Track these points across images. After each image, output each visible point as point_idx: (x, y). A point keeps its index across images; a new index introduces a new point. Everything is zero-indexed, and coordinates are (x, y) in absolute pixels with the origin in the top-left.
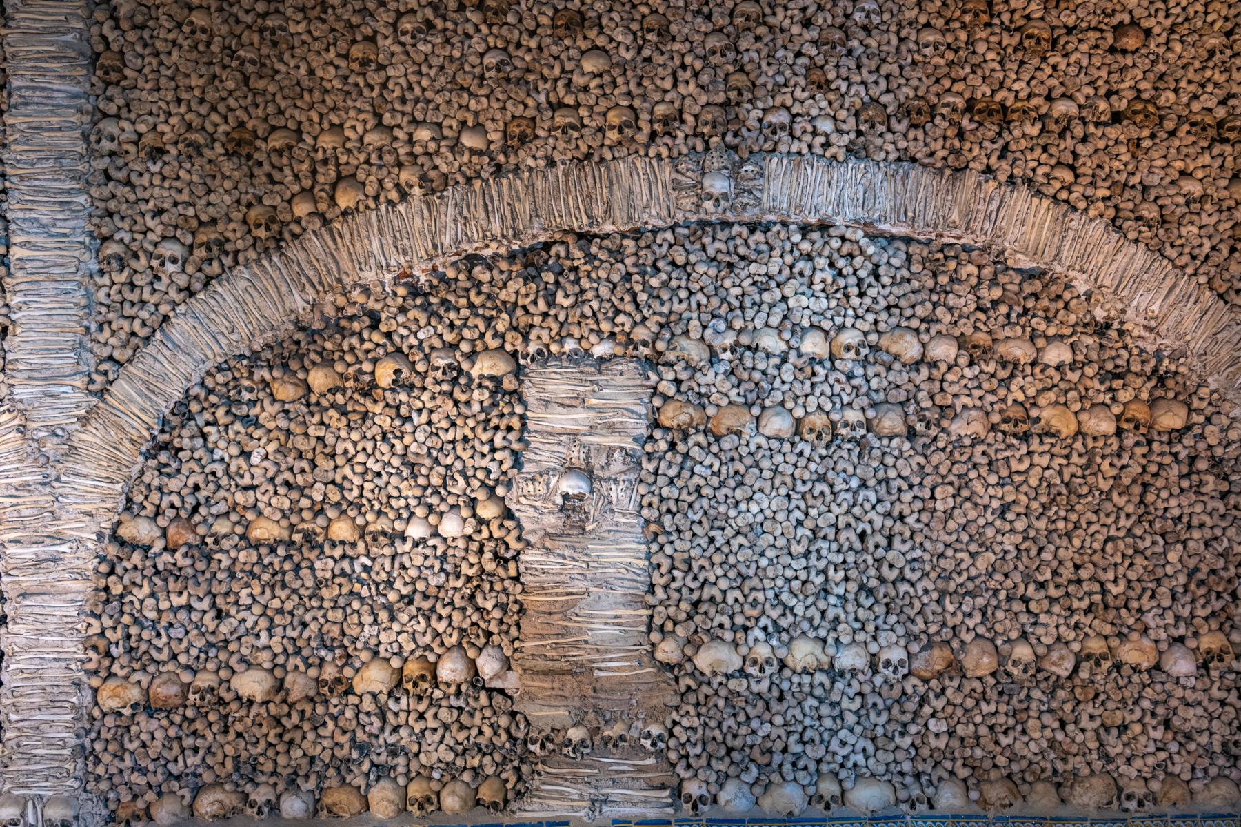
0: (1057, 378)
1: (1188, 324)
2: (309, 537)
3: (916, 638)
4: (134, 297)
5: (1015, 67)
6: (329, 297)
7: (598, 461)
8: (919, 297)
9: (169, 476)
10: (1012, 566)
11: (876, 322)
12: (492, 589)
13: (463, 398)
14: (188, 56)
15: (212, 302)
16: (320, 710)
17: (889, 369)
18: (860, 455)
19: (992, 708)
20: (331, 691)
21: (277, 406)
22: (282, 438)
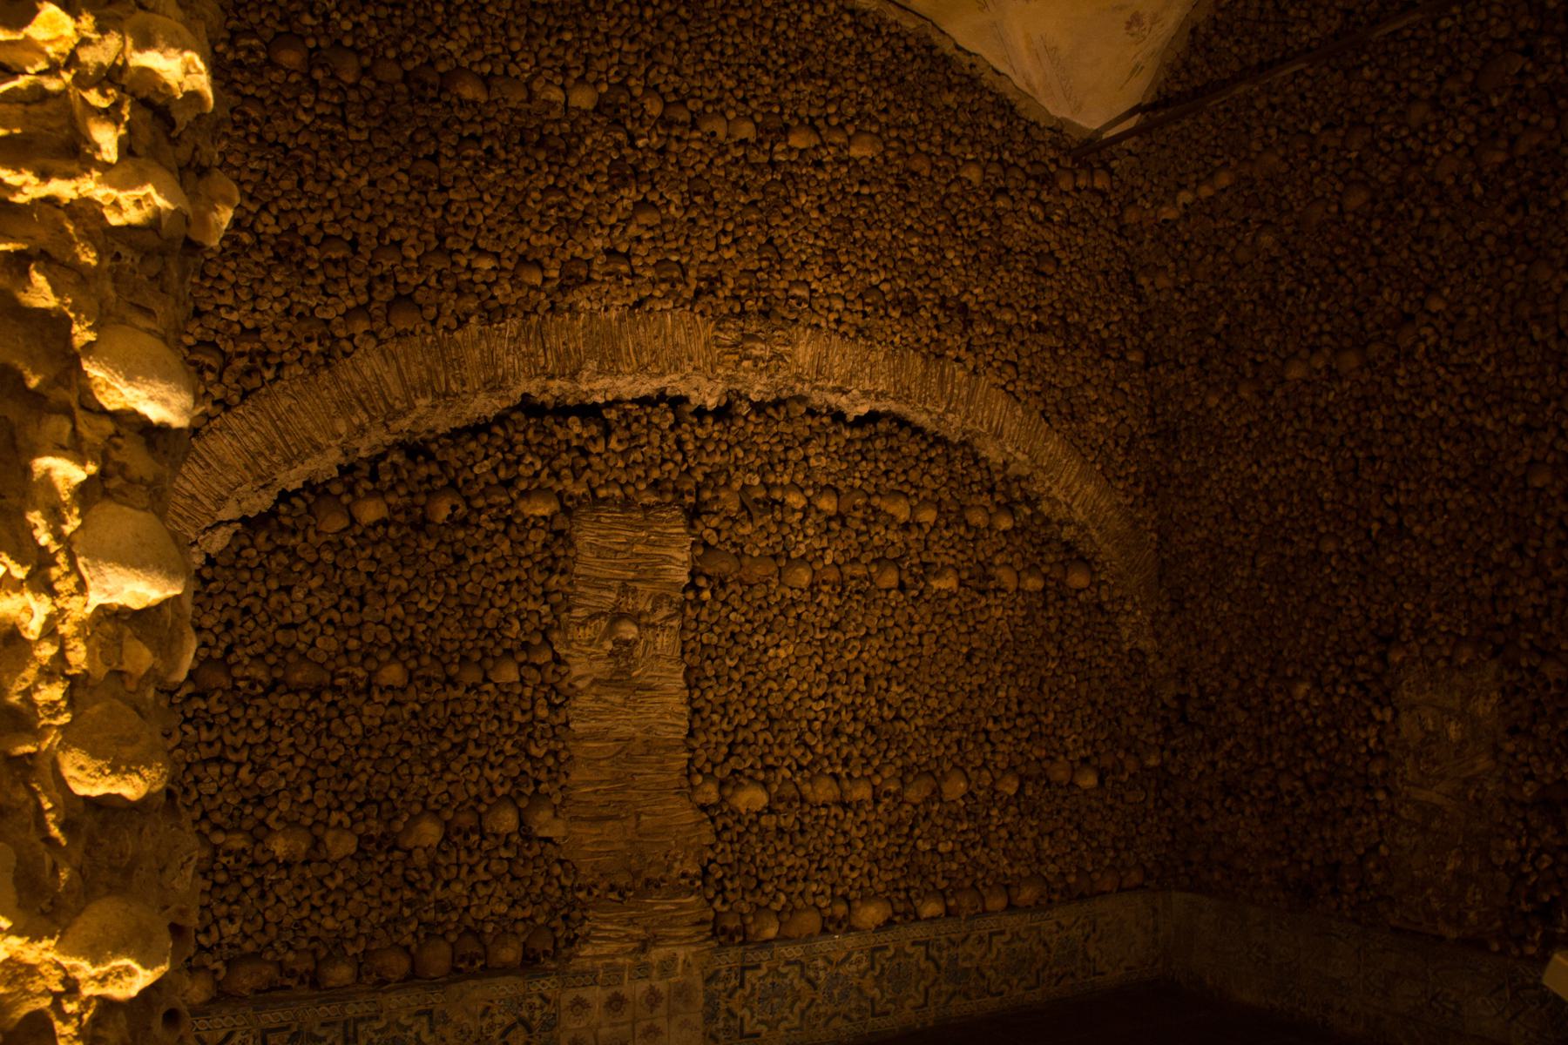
15: (253, 418)
19: (965, 827)
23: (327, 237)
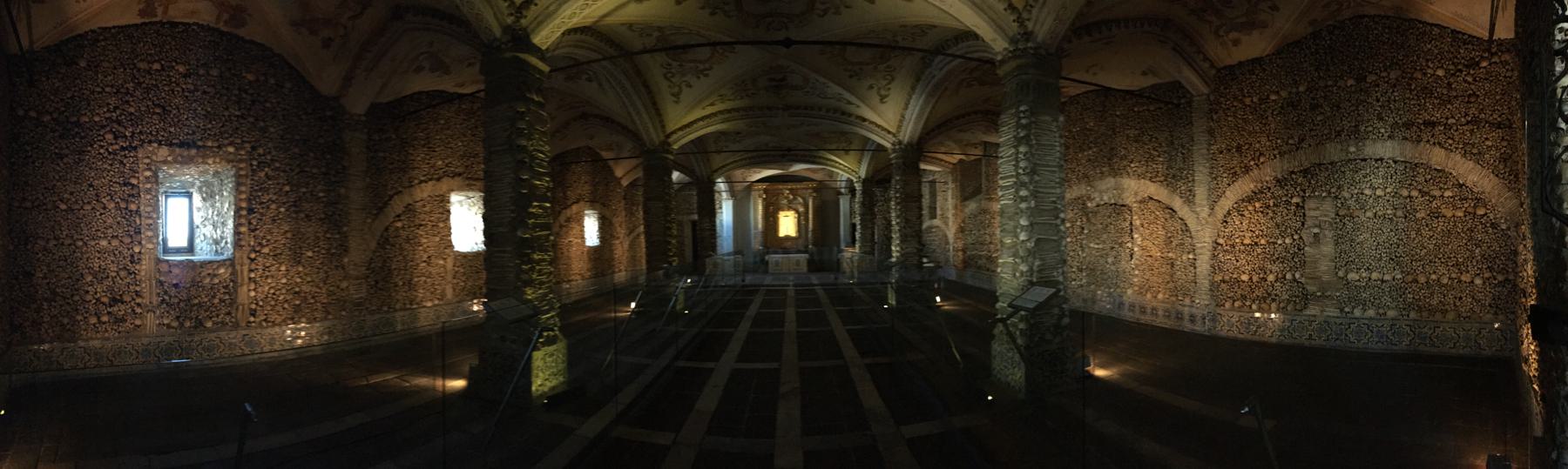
2: (1256, 243)
7: (1322, 224)
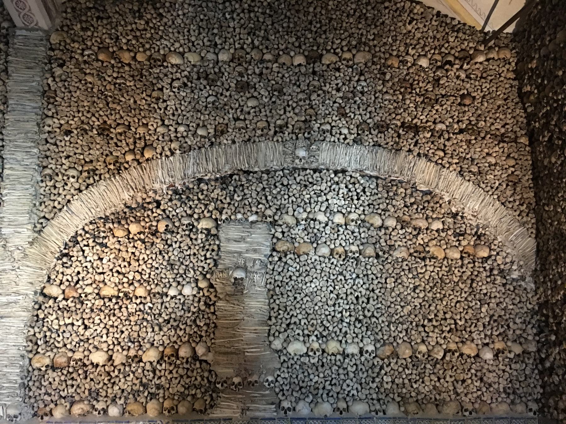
0: (437, 235)
1: (490, 215)
2: (126, 295)
3: (379, 341)
4: (56, 192)
5: (421, 110)
6: (140, 194)
7: (250, 265)
8: (381, 201)
9: (67, 267)
10: (418, 311)
11: (364, 211)
12: (203, 317)
13: (194, 237)
14: (84, 93)
15: (89, 195)
16: (127, 369)
17: (369, 229)
18: (356, 265)
20: (133, 361)
21: (115, 239)
22: (117, 253)
23: (119, 124)
